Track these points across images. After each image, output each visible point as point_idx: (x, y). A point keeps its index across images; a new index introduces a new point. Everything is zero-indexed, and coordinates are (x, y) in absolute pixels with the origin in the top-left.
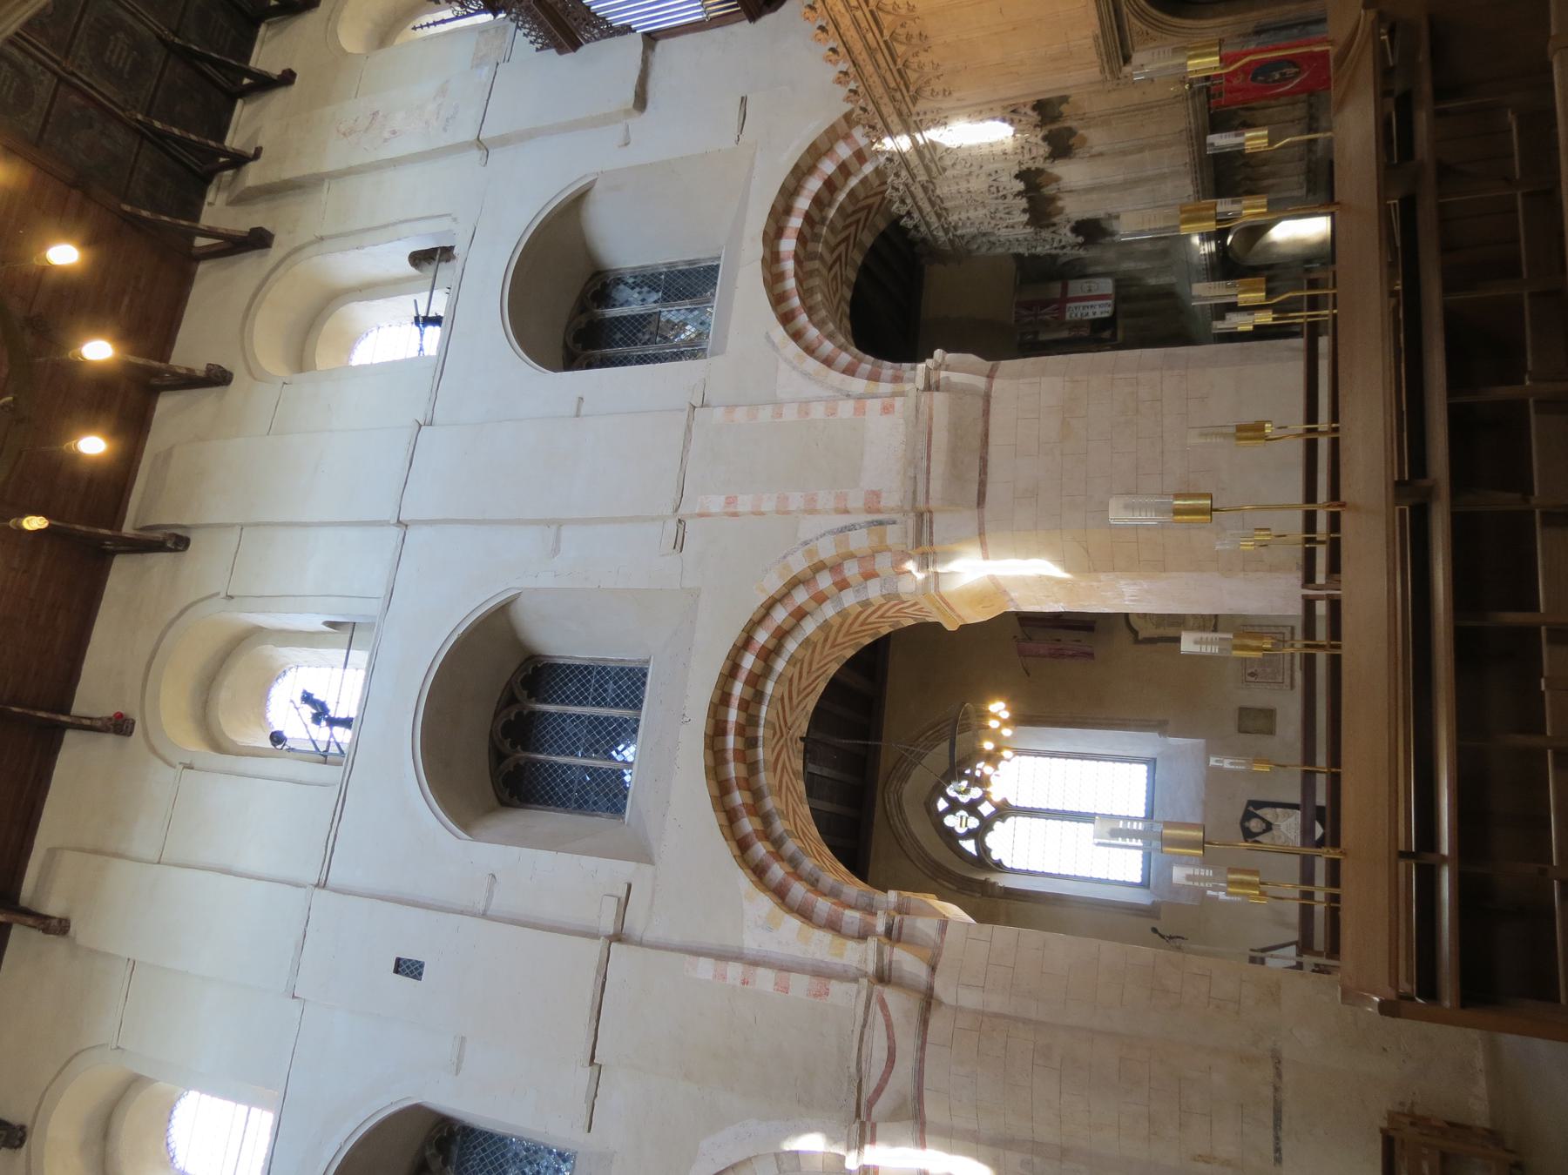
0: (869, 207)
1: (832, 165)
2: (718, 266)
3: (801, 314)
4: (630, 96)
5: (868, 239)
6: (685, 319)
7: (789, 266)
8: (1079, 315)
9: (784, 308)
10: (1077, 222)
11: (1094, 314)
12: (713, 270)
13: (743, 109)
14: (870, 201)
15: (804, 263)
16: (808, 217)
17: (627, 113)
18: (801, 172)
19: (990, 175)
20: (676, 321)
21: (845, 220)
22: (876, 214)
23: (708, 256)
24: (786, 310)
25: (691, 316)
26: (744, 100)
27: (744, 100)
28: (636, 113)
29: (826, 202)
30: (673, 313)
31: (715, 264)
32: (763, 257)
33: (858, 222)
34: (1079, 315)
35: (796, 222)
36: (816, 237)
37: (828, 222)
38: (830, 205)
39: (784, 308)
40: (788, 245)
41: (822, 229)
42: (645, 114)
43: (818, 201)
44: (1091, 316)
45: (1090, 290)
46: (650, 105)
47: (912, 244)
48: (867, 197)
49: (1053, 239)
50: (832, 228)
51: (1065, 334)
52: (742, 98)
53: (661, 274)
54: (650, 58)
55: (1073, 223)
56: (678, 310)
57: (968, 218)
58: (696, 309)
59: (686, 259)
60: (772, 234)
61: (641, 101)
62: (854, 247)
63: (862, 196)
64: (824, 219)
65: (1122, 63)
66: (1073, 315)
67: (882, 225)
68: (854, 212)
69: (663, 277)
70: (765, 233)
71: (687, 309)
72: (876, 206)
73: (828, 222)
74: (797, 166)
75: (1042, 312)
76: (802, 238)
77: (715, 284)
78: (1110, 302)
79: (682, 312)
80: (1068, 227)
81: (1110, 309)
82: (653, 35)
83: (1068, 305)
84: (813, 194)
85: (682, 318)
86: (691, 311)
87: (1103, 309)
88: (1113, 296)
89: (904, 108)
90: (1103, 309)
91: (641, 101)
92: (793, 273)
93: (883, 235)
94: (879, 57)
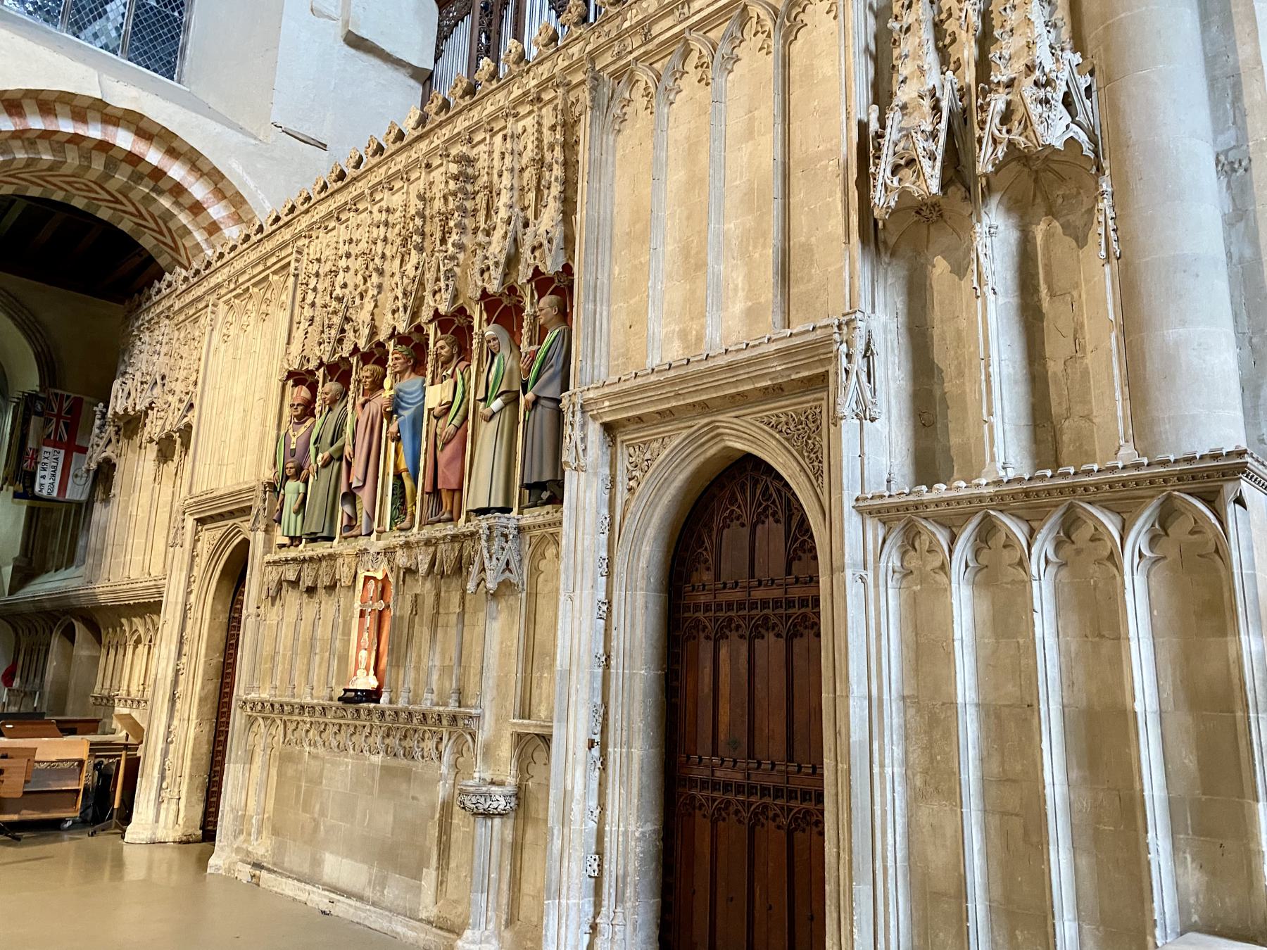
0: (176, 249)
1: (219, 216)
2: (172, 78)
3: (15, 125)
4: (363, 33)
5: (147, 242)
6: (108, 19)
7: (94, 132)
8: (46, 461)
9: (28, 105)
10: (114, 465)
11: (43, 477)
12: (168, 71)
13: (312, 142)
14: (183, 252)
15: (105, 155)
16: (158, 174)
17: (346, 23)
18: (215, 177)
19: (163, 378)
20: (108, 7)
21: (160, 217)
22: (172, 257)
23: (185, 70)
24: (26, 109)
25: (110, 26)
26: (323, 146)
27: (323, 146)
28: (344, 33)
29: (181, 200)
30: (122, 7)
31: (175, 76)
32: (109, 105)
33: (161, 233)
34: (46, 461)
35: (154, 156)
36: (137, 178)
37: (154, 195)
38: (176, 203)
39: (28, 105)
40: (124, 140)
41: (147, 187)
42: (342, 43)
43: (178, 190)
44: (39, 473)
45: (76, 476)
46: (353, 51)
47: (140, 292)
48: (185, 248)
49: (102, 438)
50: (147, 199)
51: (31, 444)
52: (325, 146)
53: (180, 13)
54: (403, 70)
55: (115, 460)
56: (123, 15)
57: (141, 352)
58: (120, 35)
59: (189, 46)
60: (142, 124)
61: (356, 42)
62: (136, 223)
63: (188, 244)
64: (161, 192)
65: (197, 516)
66: (47, 455)
67: (163, 261)
68: (169, 230)
69: (176, 14)
70: (142, 116)
71: (121, 25)
72: (180, 259)
73: (154, 195)
74: (223, 177)
75: (62, 424)
76: (133, 159)
77: (129, 60)
78: (55, 494)
79: (120, 19)
80: (113, 456)
81: (45, 493)
82: (428, 82)
83: (63, 452)
84: (186, 186)
85: (111, 15)
86: (117, 29)
87: (46, 487)
88: (60, 499)
89: (223, 291)
90: (46, 487)
91: (356, 42)
92: (81, 132)
93: (151, 260)
94: (261, 268)
